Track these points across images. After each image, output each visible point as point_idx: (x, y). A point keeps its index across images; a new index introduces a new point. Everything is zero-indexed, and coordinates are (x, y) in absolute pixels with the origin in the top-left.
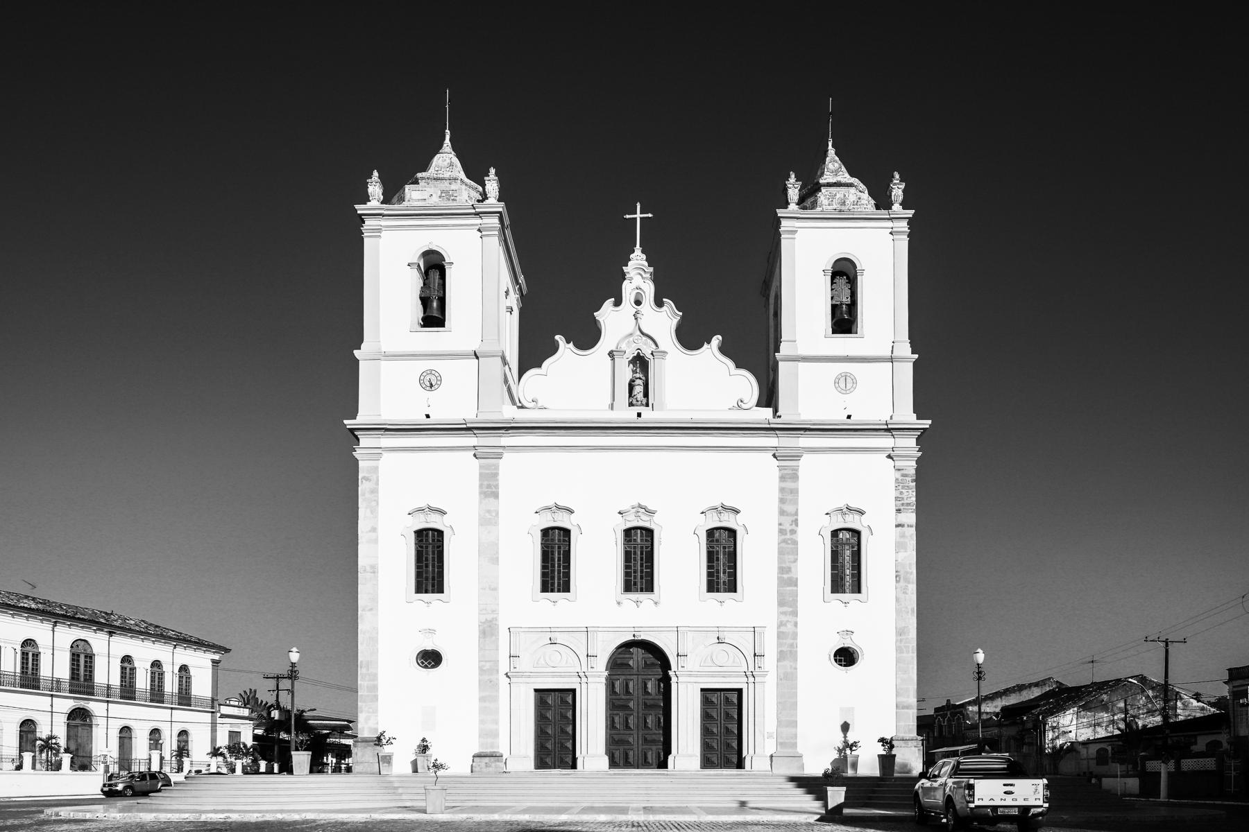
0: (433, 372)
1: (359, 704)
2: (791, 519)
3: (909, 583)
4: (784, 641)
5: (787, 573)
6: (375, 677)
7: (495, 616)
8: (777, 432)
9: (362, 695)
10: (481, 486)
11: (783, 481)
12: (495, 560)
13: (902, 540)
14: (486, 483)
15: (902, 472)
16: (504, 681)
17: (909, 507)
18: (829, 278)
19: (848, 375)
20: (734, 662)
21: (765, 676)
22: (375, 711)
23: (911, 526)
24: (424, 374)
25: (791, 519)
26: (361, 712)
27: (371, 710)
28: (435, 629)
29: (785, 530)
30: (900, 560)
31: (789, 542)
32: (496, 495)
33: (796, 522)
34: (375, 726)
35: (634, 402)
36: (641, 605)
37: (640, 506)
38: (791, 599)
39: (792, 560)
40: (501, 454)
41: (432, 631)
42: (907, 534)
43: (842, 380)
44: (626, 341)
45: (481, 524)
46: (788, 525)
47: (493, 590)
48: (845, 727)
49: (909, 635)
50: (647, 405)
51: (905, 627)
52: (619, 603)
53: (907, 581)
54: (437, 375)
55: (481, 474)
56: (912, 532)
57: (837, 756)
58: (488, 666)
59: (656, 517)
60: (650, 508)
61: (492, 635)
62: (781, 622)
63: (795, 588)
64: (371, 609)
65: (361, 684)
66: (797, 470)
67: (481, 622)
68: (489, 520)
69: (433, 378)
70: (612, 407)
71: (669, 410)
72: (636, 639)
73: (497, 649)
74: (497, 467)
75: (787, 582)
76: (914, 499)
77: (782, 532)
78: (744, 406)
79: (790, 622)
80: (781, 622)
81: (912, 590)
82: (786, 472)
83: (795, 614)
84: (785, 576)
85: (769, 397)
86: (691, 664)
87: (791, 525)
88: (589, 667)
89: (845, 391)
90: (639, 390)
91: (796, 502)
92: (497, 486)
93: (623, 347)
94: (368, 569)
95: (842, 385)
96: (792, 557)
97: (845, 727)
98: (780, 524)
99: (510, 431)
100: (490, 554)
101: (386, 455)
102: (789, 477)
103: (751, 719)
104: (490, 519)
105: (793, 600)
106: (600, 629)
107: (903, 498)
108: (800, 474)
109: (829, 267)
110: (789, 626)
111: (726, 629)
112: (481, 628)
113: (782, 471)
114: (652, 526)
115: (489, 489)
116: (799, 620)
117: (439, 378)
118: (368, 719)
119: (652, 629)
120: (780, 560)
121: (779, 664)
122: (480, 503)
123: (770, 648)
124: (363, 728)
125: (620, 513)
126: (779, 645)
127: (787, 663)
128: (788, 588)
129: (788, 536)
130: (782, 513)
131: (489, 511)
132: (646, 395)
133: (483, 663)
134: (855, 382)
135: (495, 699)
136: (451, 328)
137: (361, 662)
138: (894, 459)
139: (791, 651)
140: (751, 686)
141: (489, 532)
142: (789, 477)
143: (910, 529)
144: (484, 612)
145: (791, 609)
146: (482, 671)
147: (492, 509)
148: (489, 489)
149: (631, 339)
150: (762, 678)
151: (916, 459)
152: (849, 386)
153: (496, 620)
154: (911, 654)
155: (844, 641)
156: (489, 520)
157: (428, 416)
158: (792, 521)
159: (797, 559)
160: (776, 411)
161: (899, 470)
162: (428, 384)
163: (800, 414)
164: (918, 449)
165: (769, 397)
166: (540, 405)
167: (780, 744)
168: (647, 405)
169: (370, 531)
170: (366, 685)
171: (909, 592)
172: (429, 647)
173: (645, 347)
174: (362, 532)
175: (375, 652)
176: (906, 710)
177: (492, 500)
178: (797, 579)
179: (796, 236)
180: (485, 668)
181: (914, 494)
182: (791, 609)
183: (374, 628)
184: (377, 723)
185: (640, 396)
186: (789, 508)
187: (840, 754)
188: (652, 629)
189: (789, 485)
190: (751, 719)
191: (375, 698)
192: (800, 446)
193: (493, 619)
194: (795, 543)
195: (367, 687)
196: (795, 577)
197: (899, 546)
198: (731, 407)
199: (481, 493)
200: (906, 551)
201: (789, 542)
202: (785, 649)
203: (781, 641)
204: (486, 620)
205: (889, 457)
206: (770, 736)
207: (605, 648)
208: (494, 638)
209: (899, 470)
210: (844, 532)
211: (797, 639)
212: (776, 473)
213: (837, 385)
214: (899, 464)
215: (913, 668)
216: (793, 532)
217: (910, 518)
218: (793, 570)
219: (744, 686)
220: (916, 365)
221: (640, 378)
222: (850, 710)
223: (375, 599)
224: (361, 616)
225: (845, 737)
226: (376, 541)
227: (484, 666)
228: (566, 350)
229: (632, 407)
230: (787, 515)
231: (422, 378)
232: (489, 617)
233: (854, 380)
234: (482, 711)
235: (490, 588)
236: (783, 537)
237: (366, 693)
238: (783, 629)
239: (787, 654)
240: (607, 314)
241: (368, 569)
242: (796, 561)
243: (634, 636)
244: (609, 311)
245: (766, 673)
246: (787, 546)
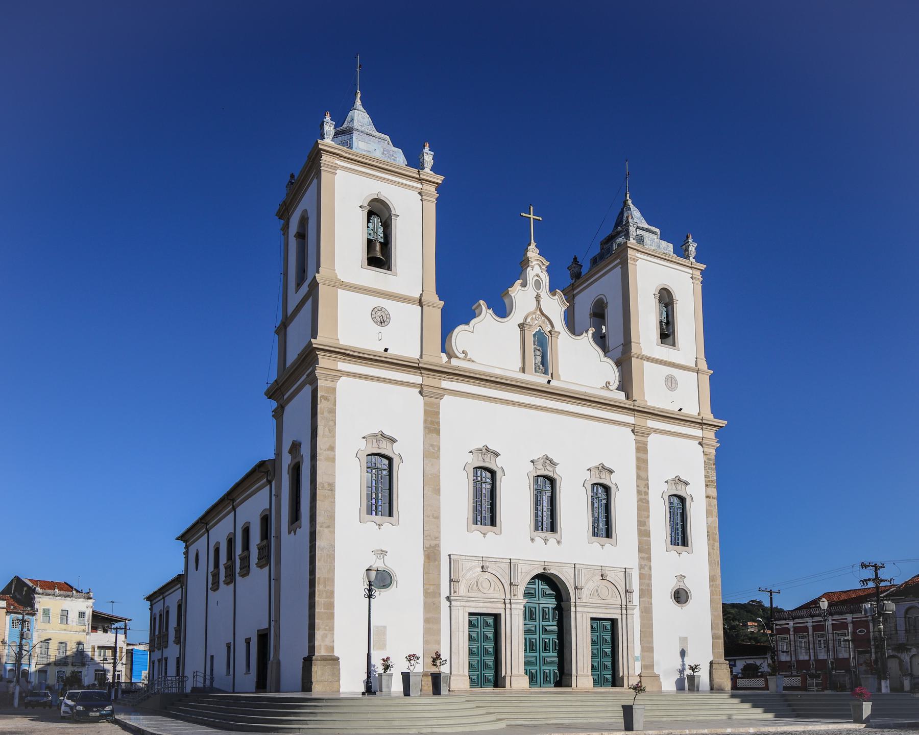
1: (316, 621)
2: (644, 483)
3: (715, 541)
4: (644, 581)
5: (644, 526)
6: (331, 594)
7: (437, 542)
8: (636, 413)
9: (318, 612)
10: (425, 421)
11: (638, 452)
12: (437, 491)
13: (709, 508)
14: (429, 419)
15: (707, 456)
16: (445, 604)
17: (713, 484)
20: (612, 596)
21: (633, 609)
22: (332, 629)
23: (715, 499)
25: (644, 483)
26: (319, 630)
27: (327, 628)
28: (386, 550)
29: (641, 491)
30: (709, 524)
31: (644, 501)
32: (438, 432)
33: (647, 486)
34: (332, 644)
36: (548, 543)
37: (547, 458)
38: (647, 547)
39: (646, 516)
40: (443, 396)
41: (383, 553)
42: (712, 504)
43: (669, 379)
45: (425, 456)
46: (643, 488)
47: (435, 518)
48: (683, 653)
49: (716, 582)
51: (714, 575)
52: (532, 540)
53: (714, 539)
55: (425, 411)
56: (715, 502)
57: (678, 676)
58: (432, 588)
59: (558, 469)
60: (555, 460)
61: (435, 560)
62: (641, 565)
63: (649, 539)
64: (328, 527)
65: (318, 601)
66: (647, 445)
67: (426, 548)
68: (432, 453)
70: (523, 370)
71: (562, 381)
72: (546, 572)
73: (439, 574)
74: (438, 407)
75: (644, 533)
76: (715, 478)
77: (639, 492)
78: (611, 388)
79: (647, 566)
80: (641, 565)
81: (717, 547)
82: (640, 445)
83: (649, 559)
84: (643, 528)
85: (625, 385)
86: (585, 594)
87: (645, 488)
88: (512, 595)
91: (647, 471)
92: (438, 423)
94: (326, 486)
95: (670, 384)
96: (645, 513)
97: (683, 653)
98: (638, 486)
99: (451, 377)
100: (432, 484)
101: (343, 379)
102: (642, 449)
103: (625, 645)
104: (433, 452)
105: (648, 548)
106: (520, 562)
107: (708, 476)
108: (650, 447)
110: (646, 568)
111: (607, 568)
112: (426, 553)
113: (638, 444)
114: (555, 476)
115: (432, 425)
116: (653, 564)
118: (325, 636)
119: (557, 564)
120: (639, 516)
121: (641, 599)
122: (425, 436)
123: (635, 586)
124: (320, 645)
125: (532, 461)
126: (641, 584)
127: (645, 599)
128: (645, 538)
129: (643, 497)
130: (639, 477)
131: (432, 445)
133: (427, 586)
135: (438, 621)
137: (319, 578)
138: (704, 446)
139: (648, 589)
140: (624, 617)
141: (432, 465)
142: (642, 449)
143: (714, 500)
144: (428, 538)
145: (647, 555)
146: (426, 593)
147: (435, 443)
148: (432, 425)
150: (632, 611)
151: (715, 448)
152: (674, 385)
153: (438, 546)
154: (718, 597)
155: (679, 584)
156: (432, 453)
158: (645, 485)
159: (649, 516)
160: (627, 397)
161: (706, 455)
164: (716, 441)
165: (625, 385)
167: (643, 667)
169: (328, 450)
170: (323, 602)
171: (715, 548)
172: (379, 565)
174: (321, 449)
175: (332, 570)
176: (718, 640)
177: (434, 435)
178: (650, 531)
180: (429, 591)
181: (715, 474)
182: (647, 555)
183: (332, 545)
184: (334, 641)
186: (642, 474)
187: (681, 675)
188: (557, 564)
189: (642, 455)
190: (625, 645)
191: (332, 616)
192: (648, 426)
193: (436, 545)
194: (648, 502)
195: (324, 604)
196: (648, 529)
197: (709, 513)
199: (425, 428)
200: (712, 517)
201: (644, 501)
202: (644, 588)
203: (642, 581)
204: (430, 545)
205: (700, 444)
206: (638, 660)
207: (523, 580)
208: (437, 562)
209: (706, 455)
210: (674, 497)
211: (651, 580)
212: (633, 446)
214: (706, 450)
215: (720, 607)
216: (647, 493)
217: (713, 492)
218: (647, 523)
219: (619, 617)
220: (711, 377)
221: (539, 350)
222: (684, 640)
223: (332, 517)
224: (320, 532)
225: (683, 661)
226: (333, 460)
227: (428, 589)
228: (486, 318)
230: (642, 480)
232: (433, 543)
234: (426, 632)
235: (433, 516)
236: (640, 497)
237: (322, 610)
238: (643, 571)
239: (646, 592)
241: (326, 486)
242: (648, 517)
243: (545, 569)
245: (635, 607)
246: (642, 504)
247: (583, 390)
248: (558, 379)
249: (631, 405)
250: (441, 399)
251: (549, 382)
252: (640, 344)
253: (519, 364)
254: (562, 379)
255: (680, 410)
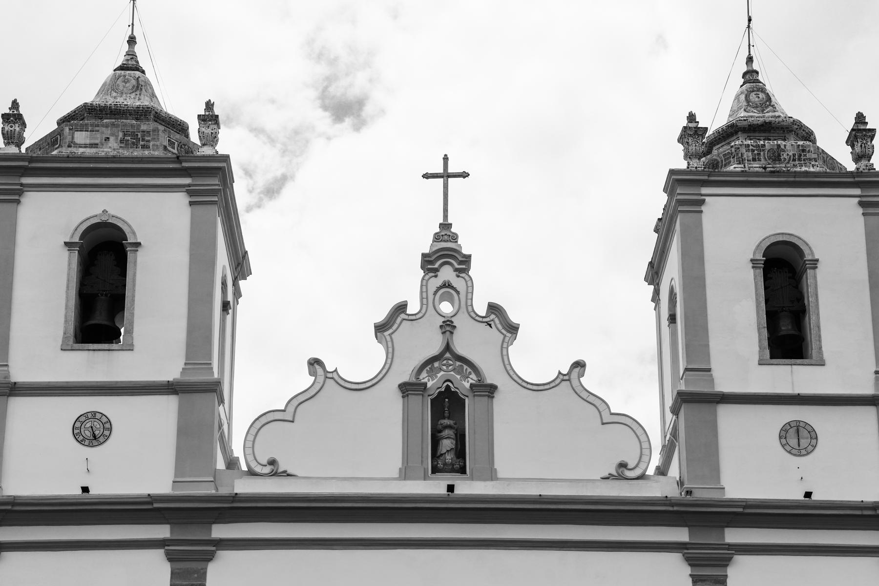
0: (98, 416)
18: (760, 272)
19: (802, 424)
24: (81, 419)
35: (440, 465)
43: (792, 431)
44: (428, 368)
50: (463, 470)
54: (104, 420)
69: (97, 425)
70: (405, 474)
78: (629, 474)
89: (799, 451)
90: (447, 444)
93: (424, 377)
95: (793, 442)
109: (760, 256)
117: (107, 426)
132: (460, 452)
134: (813, 435)
136: (132, 345)
149: (436, 364)
152: (804, 443)
157: (85, 490)
162: (88, 434)
163: (724, 488)
166: (280, 470)
168: (463, 470)
173: (458, 377)
179: (703, 208)
185: (449, 458)
198: (606, 474)
213: (784, 441)
229: (438, 475)
231: (78, 425)
233: (813, 434)
240: (394, 327)
244: (399, 320)
247: (533, 490)
248: (491, 475)
249: (665, 505)
250: (210, 560)
251: (451, 488)
252: (709, 370)
253: (399, 464)
254: (500, 475)
255: (808, 495)
